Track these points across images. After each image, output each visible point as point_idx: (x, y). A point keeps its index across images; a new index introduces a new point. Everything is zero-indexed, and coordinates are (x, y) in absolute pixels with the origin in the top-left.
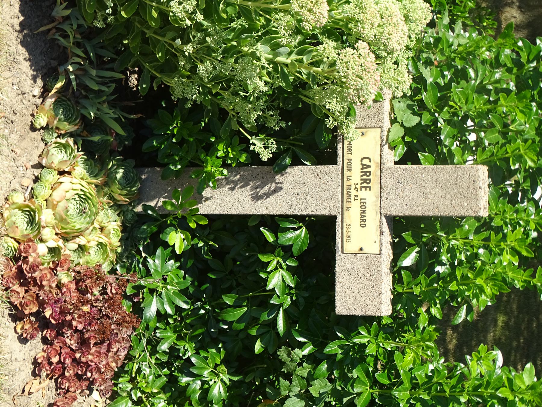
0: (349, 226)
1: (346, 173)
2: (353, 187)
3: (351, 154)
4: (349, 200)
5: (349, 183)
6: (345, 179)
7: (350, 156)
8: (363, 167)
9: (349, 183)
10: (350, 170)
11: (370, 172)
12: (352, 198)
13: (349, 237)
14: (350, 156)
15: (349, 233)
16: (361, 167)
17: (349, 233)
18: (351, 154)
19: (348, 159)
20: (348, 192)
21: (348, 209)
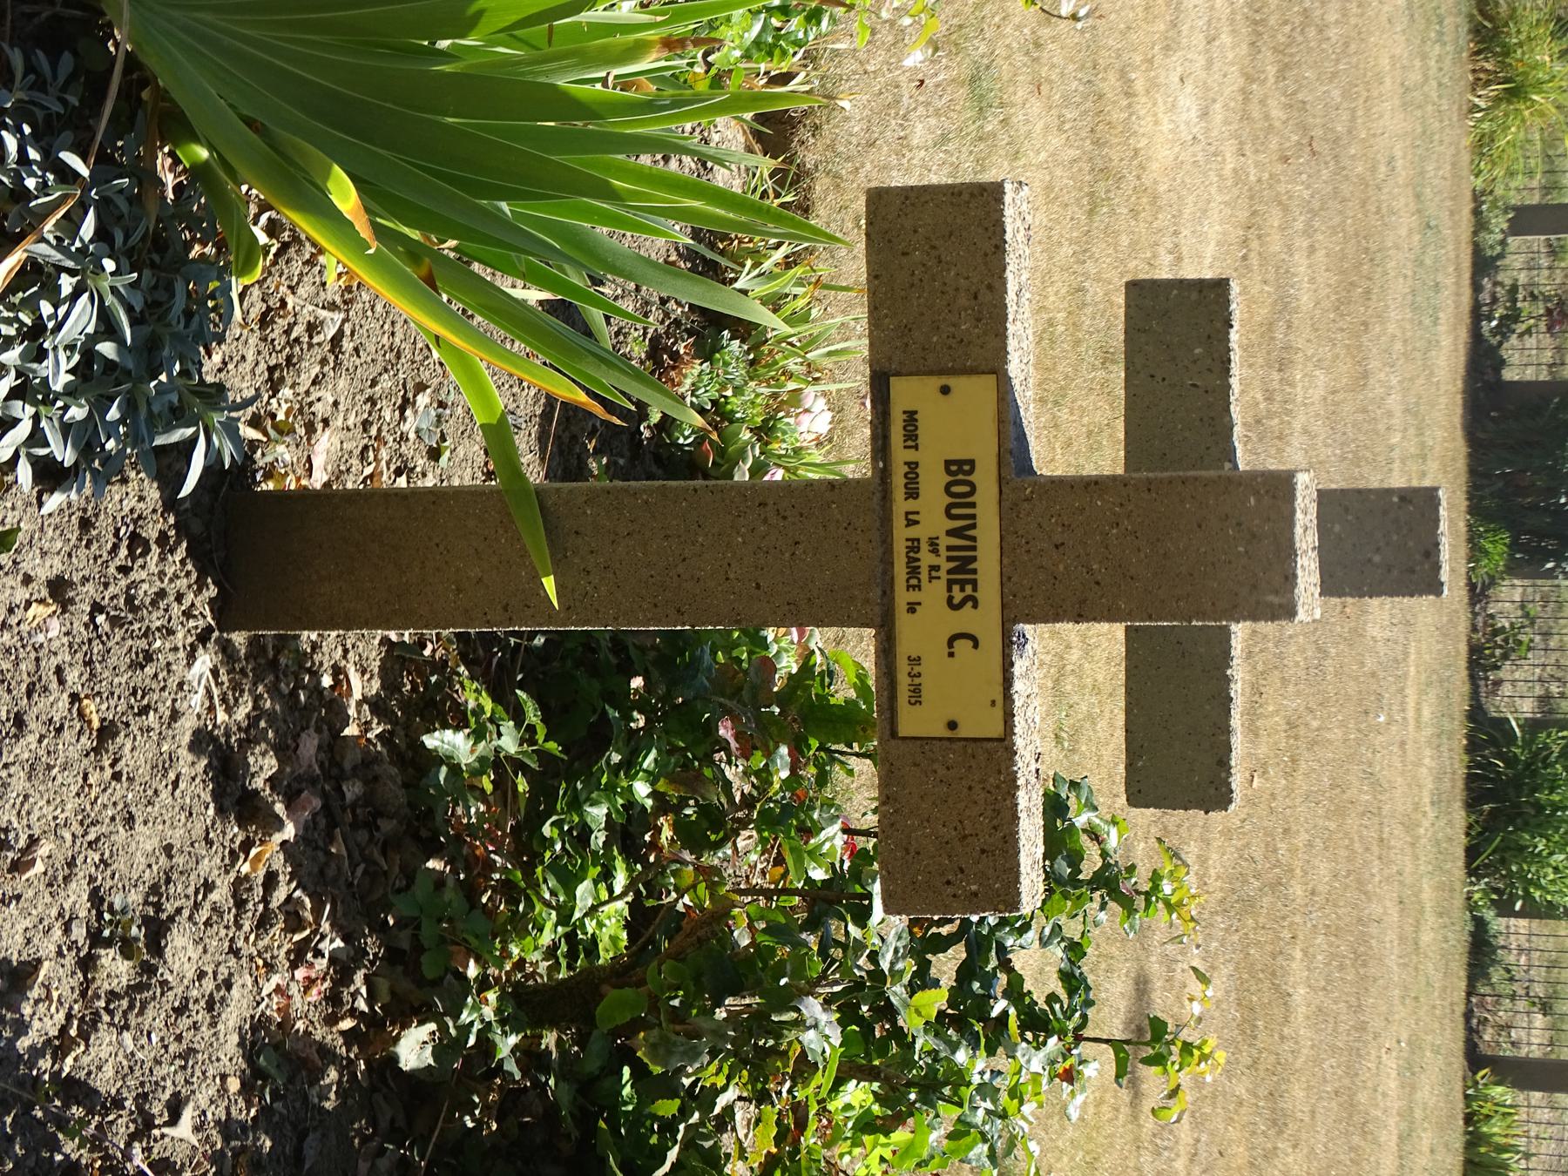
0: (915, 661)
1: (901, 505)
2: (925, 547)
3: (916, 447)
4: (914, 582)
5: (913, 532)
6: (899, 522)
7: (911, 455)
9: (913, 532)
10: (912, 493)
12: (924, 576)
13: (916, 691)
14: (911, 455)
15: (917, 681)
17: (917, 681)
18: (916, 447)
19: (907, 464)
20: (910, 560)
21: (912, 608)
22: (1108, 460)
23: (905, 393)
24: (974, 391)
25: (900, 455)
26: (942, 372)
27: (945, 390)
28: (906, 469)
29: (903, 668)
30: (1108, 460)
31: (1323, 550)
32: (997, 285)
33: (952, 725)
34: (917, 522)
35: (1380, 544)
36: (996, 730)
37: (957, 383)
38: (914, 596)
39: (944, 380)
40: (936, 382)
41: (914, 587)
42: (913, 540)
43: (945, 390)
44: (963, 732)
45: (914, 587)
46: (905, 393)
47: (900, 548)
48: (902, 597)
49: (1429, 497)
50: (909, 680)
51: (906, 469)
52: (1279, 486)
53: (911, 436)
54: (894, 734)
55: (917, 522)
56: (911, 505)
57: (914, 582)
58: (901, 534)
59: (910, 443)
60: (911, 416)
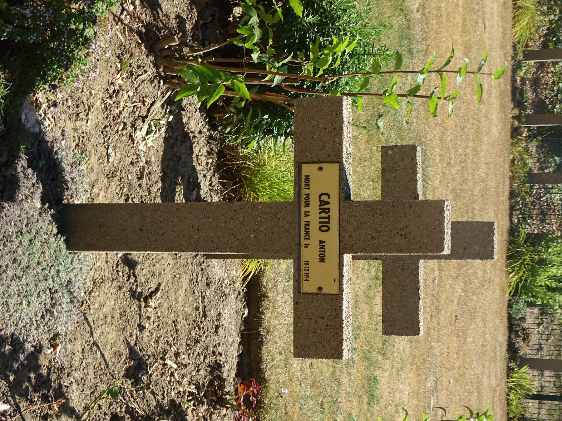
1: (304, 209)
3: (309, 188)
4: (307, 237)
5: (307, 219)
6: (303, 215)
7: (307, 191)
8: (321, 203)
9: (307, 219)
10: (307, 205)
11: (329, 209)
13: (307, 275)
14: (307, 191)
15: (307, 272)
16: (319, 203)
17: (307, 272)
18: (309, 188)
20: (306, 229)
21: (306, 246)
22: (377, 196)
23: (307, 169)
24: (331, 169)
25: (304, 191)
26: (319, 162)
27: (321, 169)
28: (305, 196)
29: (303, 266)
30: (377, 196)
31: (452, 235)
32: (340, 345)
33: (320, 289)
34: (309, 215)
35: (473, 241)
36: (336, 291)
37: (323, 165)
38: (307, 242)
39: (320, 165)
40: (317, 166)
41: (307, 238)
42: (307, 222)
43: (321, 169)
44: (324, 291)
45: (307, 238)
46: (307, 169)
47: (303, 224)
48: (304, 242)
49: (491, 225)
50: (304, 272)
51: (305, 196)
52: (437, 207)
53: (307, 185)
54: (299, 292)
55: (309, 215)
56: (307, 209)
57: (307, 237)
58: (304, 219)
59: (307, 187)
60: (307, 177)
